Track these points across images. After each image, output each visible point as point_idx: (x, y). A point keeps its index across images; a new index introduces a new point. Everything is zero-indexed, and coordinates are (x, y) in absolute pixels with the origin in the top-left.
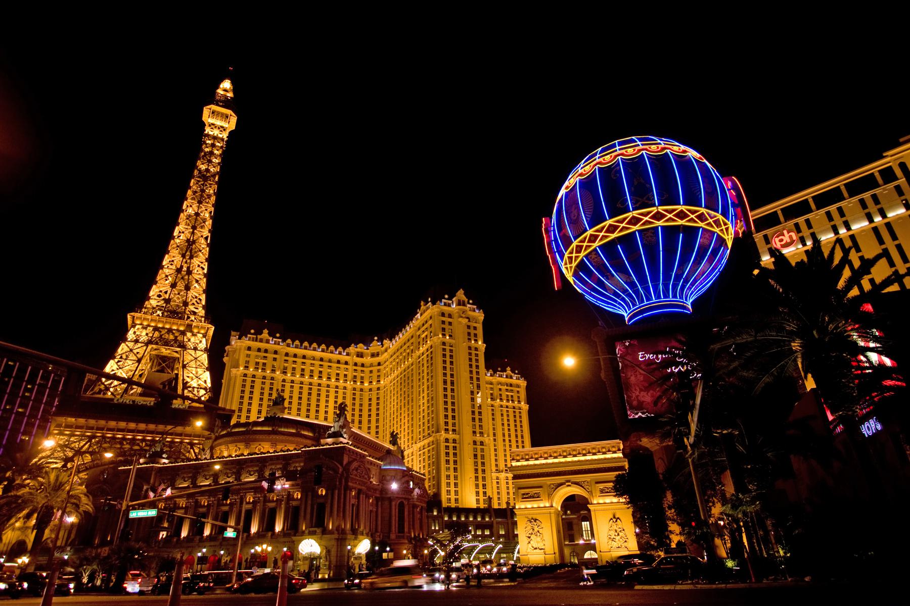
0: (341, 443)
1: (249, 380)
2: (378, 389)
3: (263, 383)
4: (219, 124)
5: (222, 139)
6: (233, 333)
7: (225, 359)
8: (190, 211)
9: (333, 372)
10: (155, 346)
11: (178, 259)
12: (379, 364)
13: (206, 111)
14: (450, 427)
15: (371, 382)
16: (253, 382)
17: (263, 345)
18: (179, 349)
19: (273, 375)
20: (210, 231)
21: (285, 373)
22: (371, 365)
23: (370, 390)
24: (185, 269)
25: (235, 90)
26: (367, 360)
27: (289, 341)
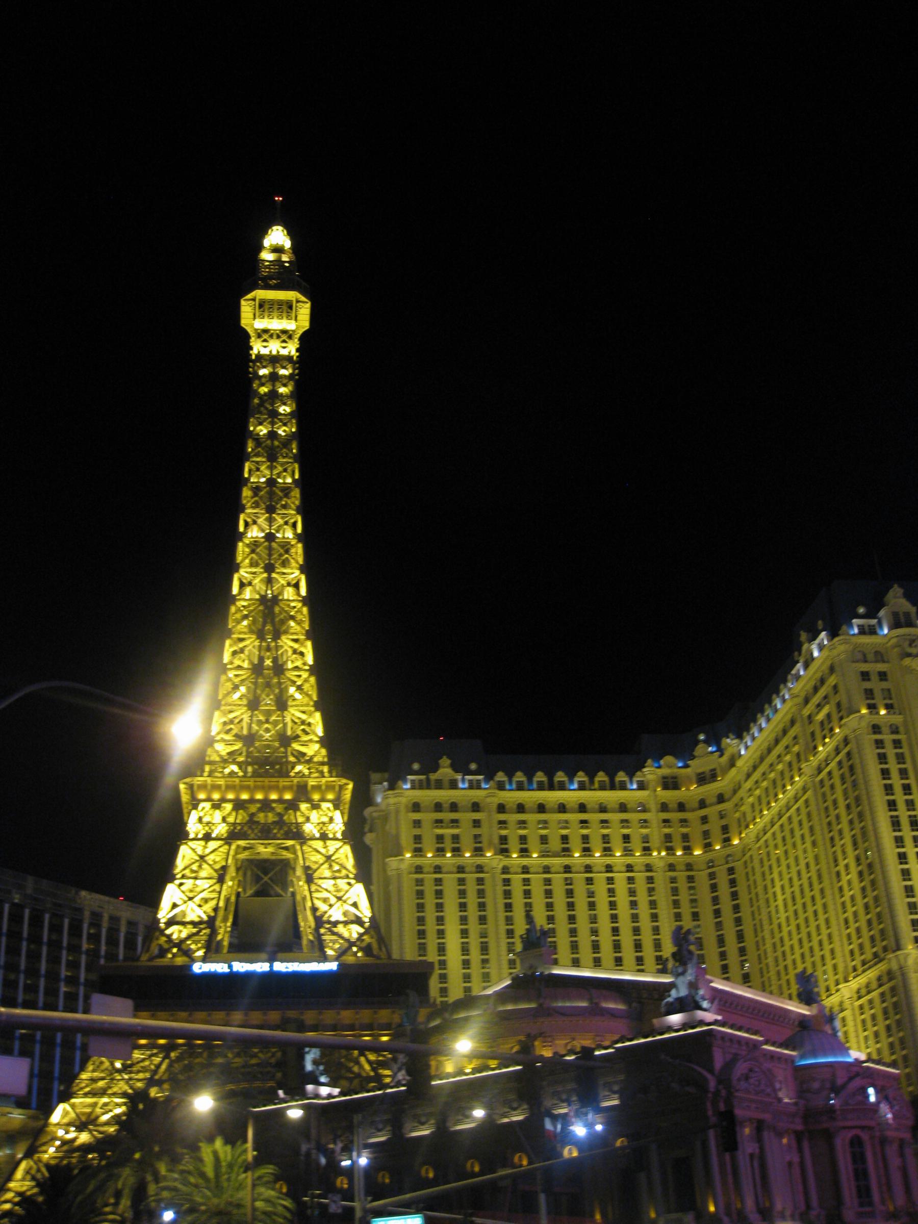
0: (702, 1023)
1: (429, 878)
3: (462, 881)
4: (274, 327)
5: (289, 359)
8: (255, 533)
9: (616, 833)
10: (242, 843)
11: (251, 643)
12: (721, 799)
13: (246, 309)
15: (708, 846)
16: (438, 882)
17: (444, 795)
18: (290, 843)
19: (479, 860)
20: (302, 569)
21: (505, 852)
22: (702, 804)
24: (268, 662)
25: (296, 248)
26: (692, 791)
27: (501, 776)
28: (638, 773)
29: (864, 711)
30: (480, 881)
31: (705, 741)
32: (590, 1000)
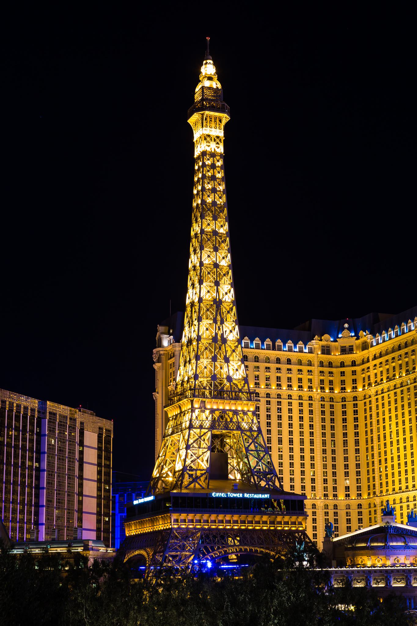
2: (355, 399)
5: (221, 155)
6: (161, 328)
7: (157, 366)
12: (354, 364)
22: (342, 365)
23: (344, 399)
24: (219, 338)
26: (336, 356)
28: (309, 343)
31: (348, 329)
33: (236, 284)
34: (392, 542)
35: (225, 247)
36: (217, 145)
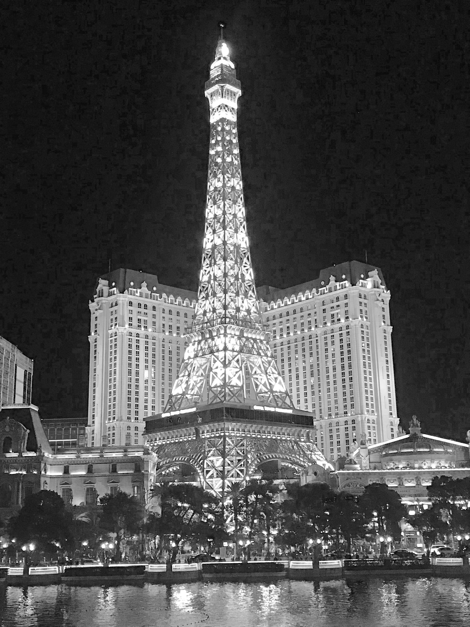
1: (134, 338)
14: (371, 409)
16: (138, 341)
24: (240, 277)
29: (360, 318)
30: (154, 344)
32: (444, 449)
33: (250, 234)
34: (435, 448)
35: (241, 202)
36: (233, 115)
